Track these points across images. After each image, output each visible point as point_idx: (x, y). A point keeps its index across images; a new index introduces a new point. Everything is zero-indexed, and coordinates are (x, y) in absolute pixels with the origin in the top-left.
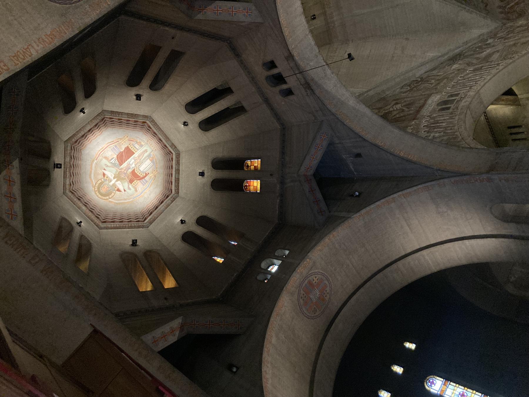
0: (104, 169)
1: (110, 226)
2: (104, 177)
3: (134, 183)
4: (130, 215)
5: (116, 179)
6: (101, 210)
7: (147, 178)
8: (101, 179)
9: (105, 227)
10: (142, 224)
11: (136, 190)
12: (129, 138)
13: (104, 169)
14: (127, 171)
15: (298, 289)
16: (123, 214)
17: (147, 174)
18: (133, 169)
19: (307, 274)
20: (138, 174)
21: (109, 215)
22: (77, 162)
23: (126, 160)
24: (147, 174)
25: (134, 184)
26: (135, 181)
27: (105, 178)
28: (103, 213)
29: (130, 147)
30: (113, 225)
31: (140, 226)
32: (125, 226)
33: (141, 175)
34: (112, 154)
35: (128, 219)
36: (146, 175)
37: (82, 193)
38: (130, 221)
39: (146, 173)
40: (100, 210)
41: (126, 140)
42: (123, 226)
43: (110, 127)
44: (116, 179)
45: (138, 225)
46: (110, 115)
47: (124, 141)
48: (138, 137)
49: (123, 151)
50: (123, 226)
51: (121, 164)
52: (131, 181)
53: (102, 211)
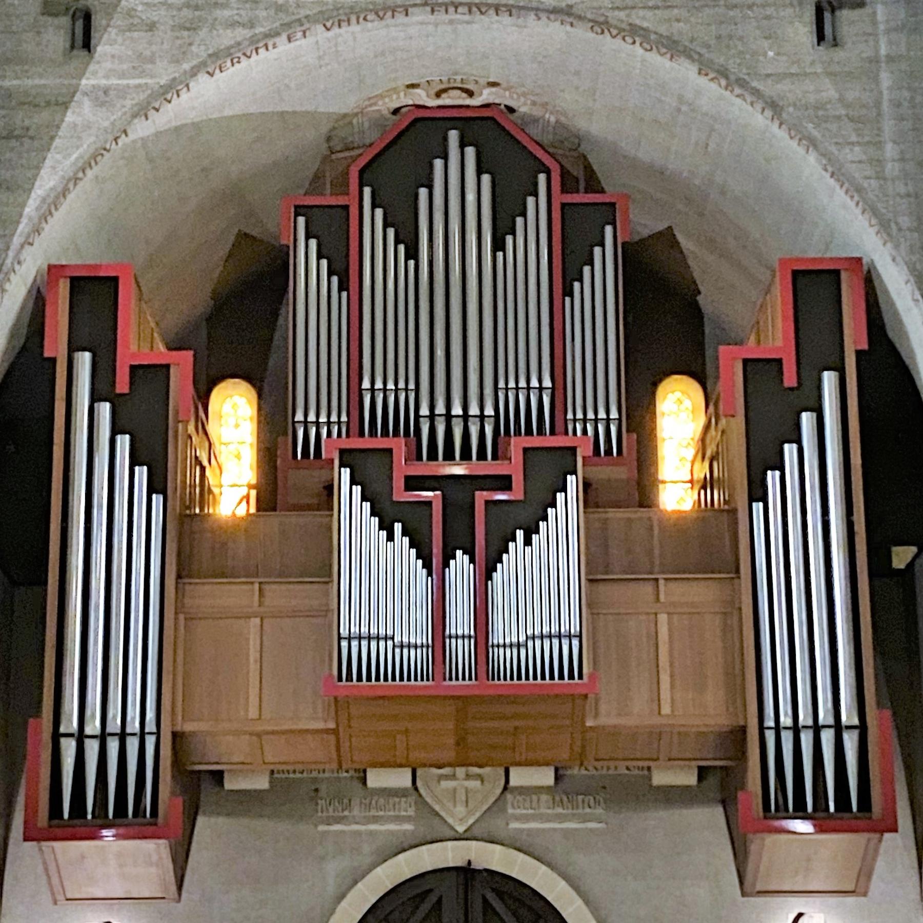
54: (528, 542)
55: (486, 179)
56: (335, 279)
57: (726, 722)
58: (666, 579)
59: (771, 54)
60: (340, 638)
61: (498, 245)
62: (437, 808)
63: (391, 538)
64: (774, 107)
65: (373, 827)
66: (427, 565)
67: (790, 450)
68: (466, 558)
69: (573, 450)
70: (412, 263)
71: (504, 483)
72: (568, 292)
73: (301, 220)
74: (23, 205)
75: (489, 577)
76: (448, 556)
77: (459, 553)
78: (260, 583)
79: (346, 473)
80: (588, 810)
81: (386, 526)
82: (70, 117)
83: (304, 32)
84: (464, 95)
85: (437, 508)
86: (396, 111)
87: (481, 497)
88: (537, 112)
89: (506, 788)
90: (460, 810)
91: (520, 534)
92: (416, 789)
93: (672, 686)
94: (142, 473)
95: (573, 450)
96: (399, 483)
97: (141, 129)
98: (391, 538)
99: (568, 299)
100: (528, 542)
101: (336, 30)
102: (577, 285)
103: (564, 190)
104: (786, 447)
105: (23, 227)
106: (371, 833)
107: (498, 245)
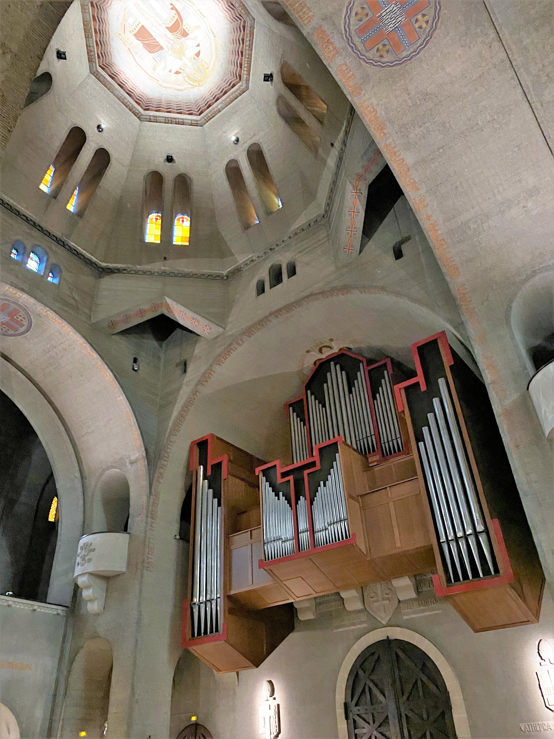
0: (170, 71)
1: (245, 76)
2: (180, 73)
3: (186, 30)
4: (233, 40)
5: (183, 57)
6: (224, 80)
7: (179, 8)
8: (184, 77)
9: (246, 83)
10: (249, 29)
11: (198, 27)
12: (121, 33)
13: (170, 71)
14: (171, 40)
15: (362, 62)
16: (231, 51)
17: (172, 6)
18: (167, 30)
19: (344, 36)
20: (173, 22)
21: (232, 71)
22: (164, 104)
23: (155, 39)
24: (172, 6)
25: (189, 30)
26: (184, 27)
27: (181, 71)
28: (228, 78)
29: (136, 31)
30: (245, 65)
31: (250, 31)
32: (249, 55)
33: (174, 17)
34: (147, 58)
35: (240, 43)
36: (174, 8)
37: (201, 102)
38: (243, 40)
39: (172, 9)
40: (224, 82)
41: (125, 38)
42: (248, 58)
43: (111, 58)
44: (183, 57)
45: (249, 36)
46: (94, 64)
47: (126, 40)
48: (118, 17)
49: (143, 43)
50: (248, 58)
51: (161, 48)
52: (185, 34)
53: (226, 79)
54: (325, 485)
55: (344, 372)
56: (302, 423)
57: (423, 545)
58: (390, 487)
59: (379, 272)
60: (264, 543)
61: (350, 392)
62: (373, 615)
63: (279, 499)
64: (383, 289)
65: (353, 627)
66: (291, 506)
67: (430, 416)
68: (304, 498)
69: (336, 443)
70: (324, 409)
71: (313, 464)
72: (374, 398)
73: (291, 408)
74: (169, 423)
75: (312, 504)
76: (297, 499)
77: (301, 497)
78: (251, 531)
79: (264, 479)
80: (433, 605)
81: (277, 495)
82: (181, 392)
83: (241, 340)
84: (329, 349)
85: (292, 483)
86: (315, 363)
87: (306, 472)
88: (357, 346)
89: (399, 601)
90: (383, 615)
91: (322, 483)
92: (366, 609)
93: (400, 535)
94: (216, 500)
95: (336, 443)
96: (279, 475)
97: (206, 390)
98: (279, 499)
99: (375, 401)
100: (325, 485)
101: (253, 337)
102: (378, 395)
103: (368, 366)
104: (429, 415)
105: (168, 430)
106: (352, 630)
107: (350, 392)
